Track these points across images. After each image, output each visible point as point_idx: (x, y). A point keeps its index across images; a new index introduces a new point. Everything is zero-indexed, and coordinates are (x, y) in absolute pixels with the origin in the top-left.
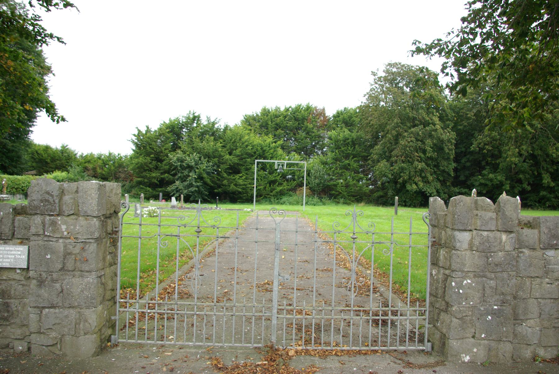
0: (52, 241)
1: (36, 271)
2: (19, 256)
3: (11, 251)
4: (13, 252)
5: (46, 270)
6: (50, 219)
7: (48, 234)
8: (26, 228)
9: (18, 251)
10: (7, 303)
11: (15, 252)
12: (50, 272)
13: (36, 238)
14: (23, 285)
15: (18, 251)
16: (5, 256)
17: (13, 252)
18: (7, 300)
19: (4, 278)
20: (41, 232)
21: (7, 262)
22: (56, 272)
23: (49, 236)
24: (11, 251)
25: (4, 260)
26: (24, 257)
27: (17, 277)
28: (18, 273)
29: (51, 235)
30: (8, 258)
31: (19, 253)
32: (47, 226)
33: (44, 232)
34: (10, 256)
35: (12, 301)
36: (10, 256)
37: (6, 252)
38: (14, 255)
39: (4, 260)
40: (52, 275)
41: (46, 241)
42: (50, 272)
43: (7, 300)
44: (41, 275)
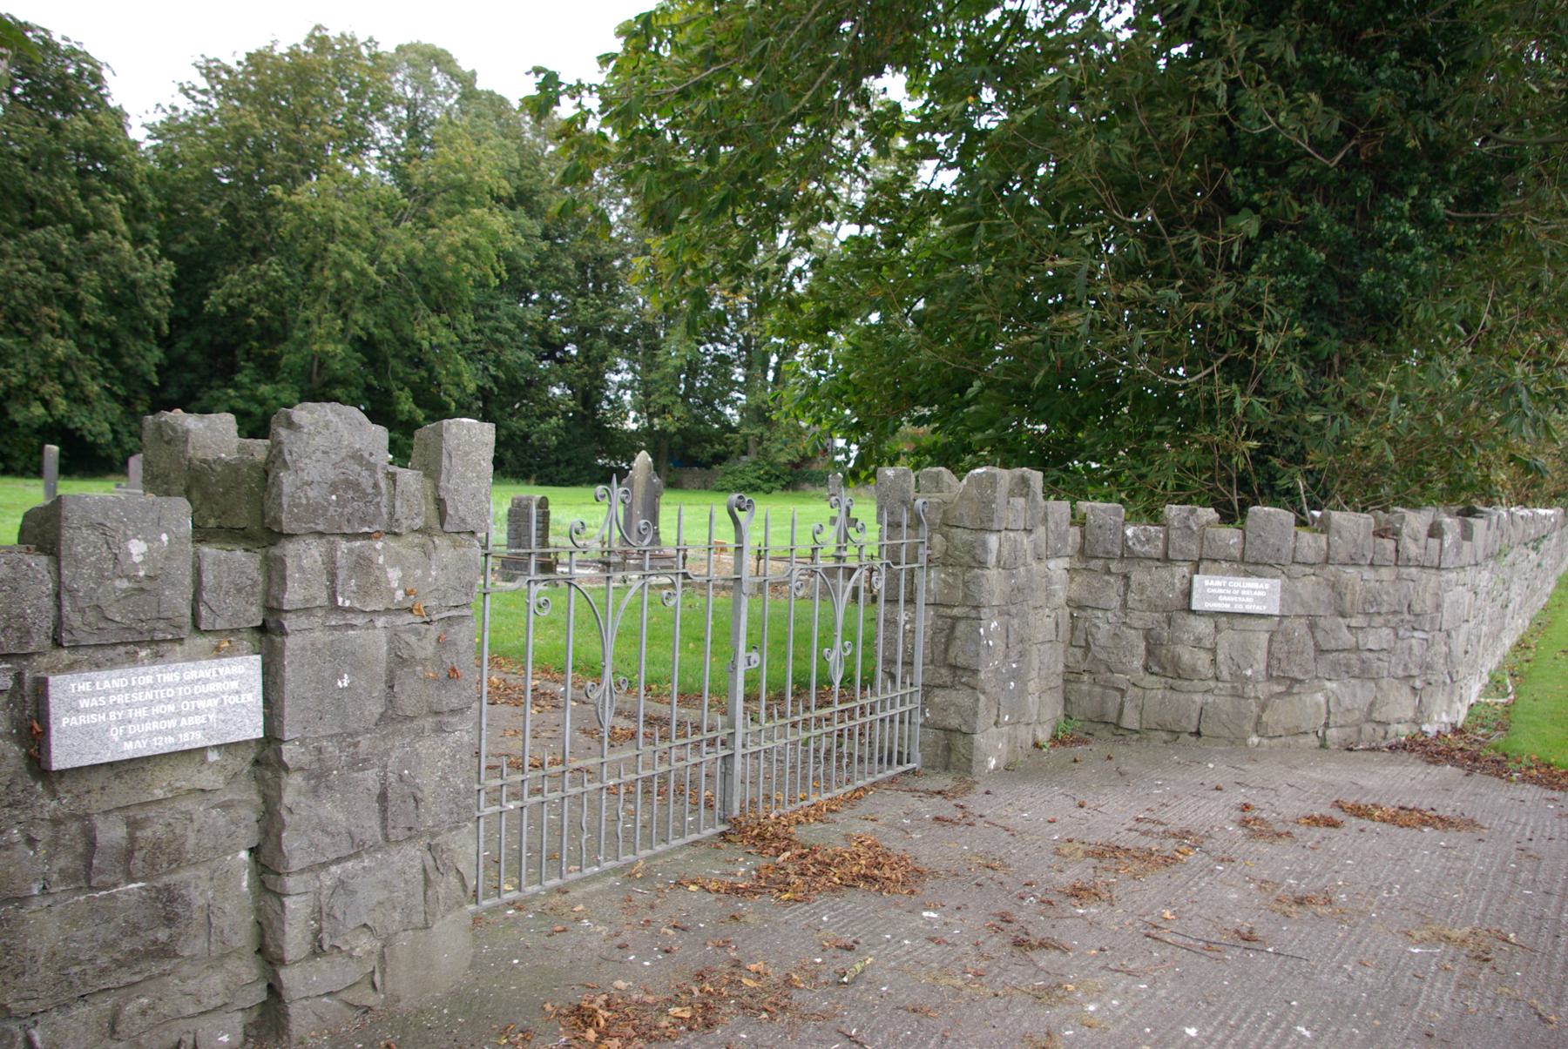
0: (352, 627)
1: (302, 744)
2: (236, 699)
3: (206, 681)
4: (211, 688)
5: (337, 730)
6: (351, 551)
7: (347, 603)
8: (239, 591)
9: (230, 678)
10: (167, 888)
11: (219, 686)
12: (350, 735)
13: (303, 622)
14: (226, 806)
15: (230, 678)
16: (187, 706)
17: (211, 688)
18: (165, 879)
19: (159, 793)
20: (323, 599)
21: (195, 728)
22: (367, 730)
23: (351, 610)
24: (206, 681)
25: (184, 722)
26: (250, 697)
27: (207, 779)
28: (211, 765)
29: (357, 605)
30: (197, 712)
31: (234, 685)
32: (342, 575)
33: (333, 597)
34: (201, 704)
35: (185, 874)
36: (201, 704)
37: (187, 691)
38: (215, 695)
39: (184, 722)
40: (356, 745)
41: (334, 628)
42: (350, 735)
43: (165, 879)
44: (320, 750)
